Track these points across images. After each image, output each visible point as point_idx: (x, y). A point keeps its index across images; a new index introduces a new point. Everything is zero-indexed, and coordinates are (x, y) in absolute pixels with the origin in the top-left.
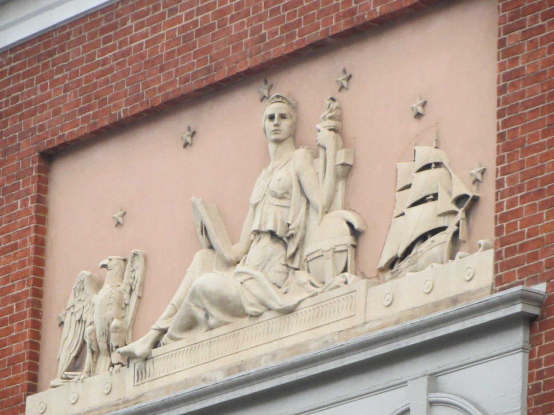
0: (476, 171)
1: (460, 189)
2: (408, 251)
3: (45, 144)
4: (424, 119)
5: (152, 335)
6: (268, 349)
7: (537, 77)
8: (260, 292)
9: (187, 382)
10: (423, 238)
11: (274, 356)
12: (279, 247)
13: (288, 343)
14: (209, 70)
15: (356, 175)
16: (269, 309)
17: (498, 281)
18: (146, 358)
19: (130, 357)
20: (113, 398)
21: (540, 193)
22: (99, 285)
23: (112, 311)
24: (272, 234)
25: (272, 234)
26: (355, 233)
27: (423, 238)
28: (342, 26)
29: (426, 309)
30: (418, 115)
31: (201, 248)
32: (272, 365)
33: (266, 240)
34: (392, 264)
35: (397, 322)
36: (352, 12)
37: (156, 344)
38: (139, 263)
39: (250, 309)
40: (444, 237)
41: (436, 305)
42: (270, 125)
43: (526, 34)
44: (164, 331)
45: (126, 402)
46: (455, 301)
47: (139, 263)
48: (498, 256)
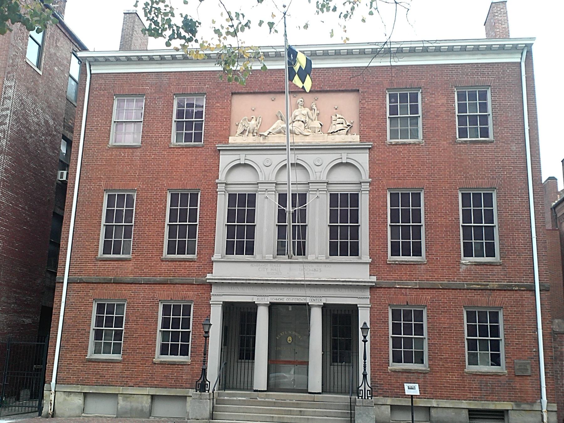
0: (352, 121)
1: (348, 124)
2: (337, 131)
3: (233, 91)
4: (337, 110)
5: (268, 132)
6: (303, 141)
7: (369, 109)
8: (300, 131)
9: (278, 143)
10: (340, 130)
11: (303, 142)
12: (303, 124)
13: (307, 141)
14: (282, 89)
15: (320, 116)
16: (301, 134)
17: (360, 141)
18: (266, 136)
19: (263, 135)
20: (256, 141)
21: (371, 128)
22: (250, 121)
23: (255, 126)
24: (302, 121)
25: (302, 121)
26: (321, 125)
27: (340, 130)
28: (319, 89)
29: (343, 142)
30: (336, 109)
31: (278, 119)
32: (302, 144)
33: (301, 122)
34: (332, 133)
35: (336, 143)
36: (322, 88)
37: (268, 134)
38: (261, 119)
39: (297, 133)
40: (345, 131)
41: (346, 142)
42: (301, 102)
43: (366, 102)
44: (270, 132)
45: (261, 143)
46: (350, 142)
47: (261, 119)
48: (360, 137)
